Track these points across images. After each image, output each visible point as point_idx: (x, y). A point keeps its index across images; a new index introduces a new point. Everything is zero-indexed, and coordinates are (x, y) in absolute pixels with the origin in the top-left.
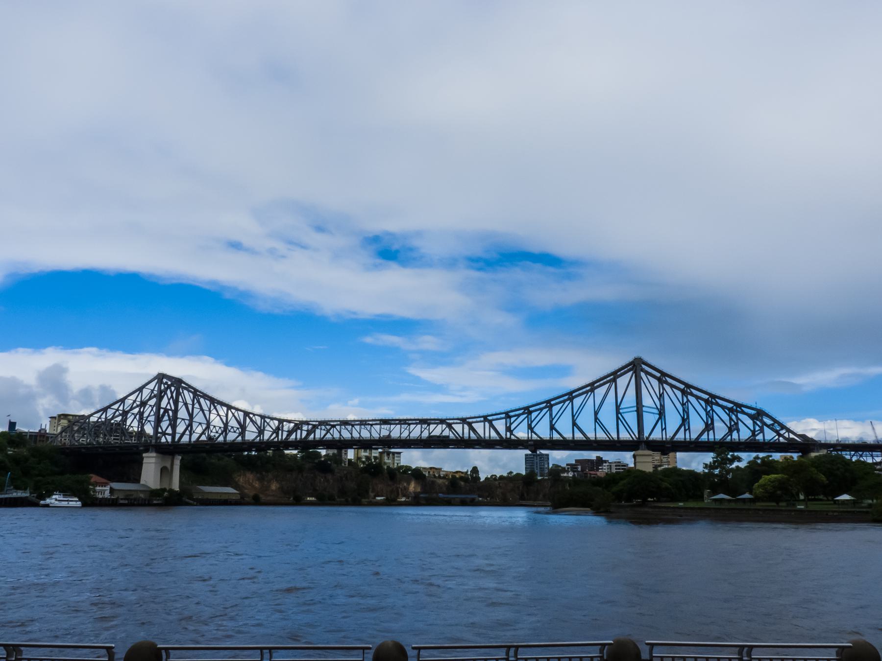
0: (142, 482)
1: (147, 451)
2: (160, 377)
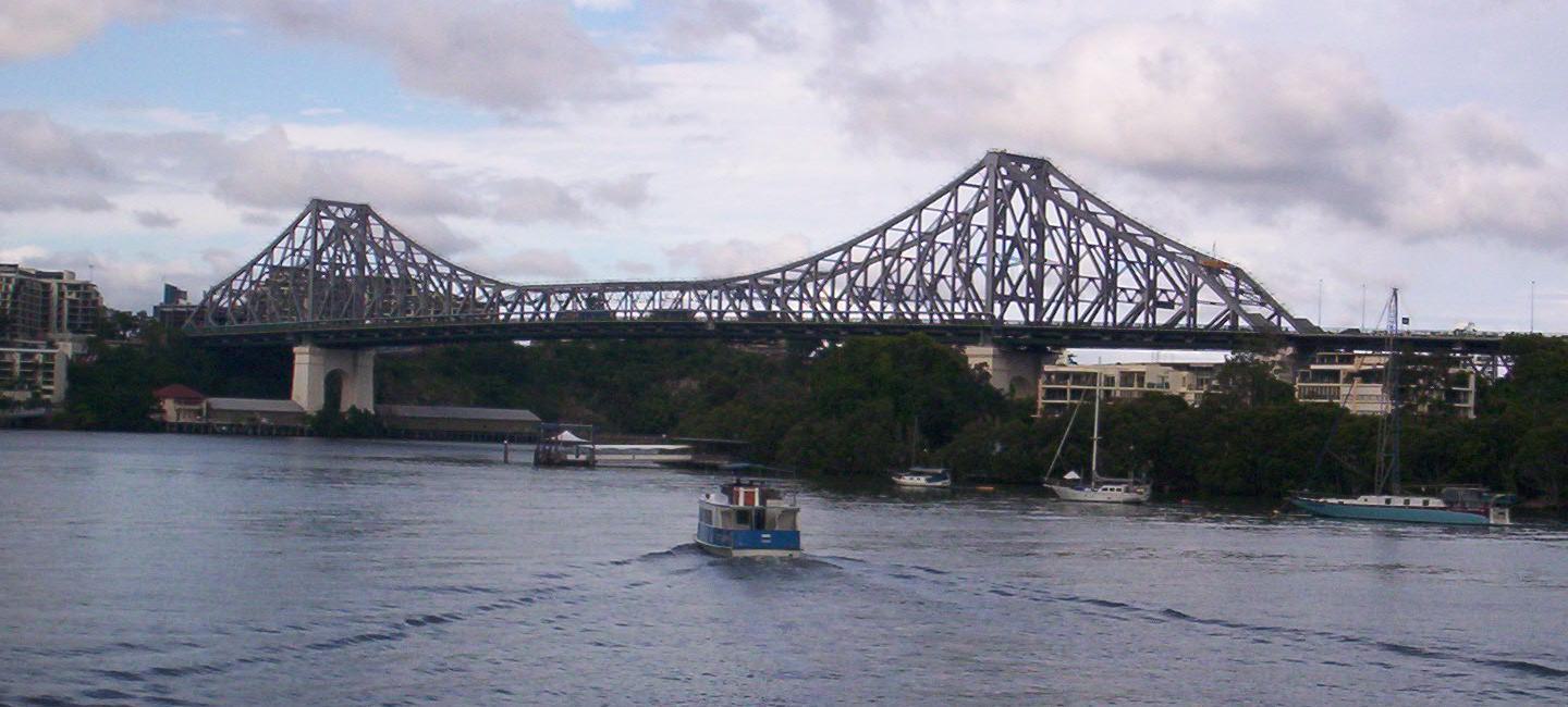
0: (294, 398)
1: (299, 342)
2: (318, 207)
